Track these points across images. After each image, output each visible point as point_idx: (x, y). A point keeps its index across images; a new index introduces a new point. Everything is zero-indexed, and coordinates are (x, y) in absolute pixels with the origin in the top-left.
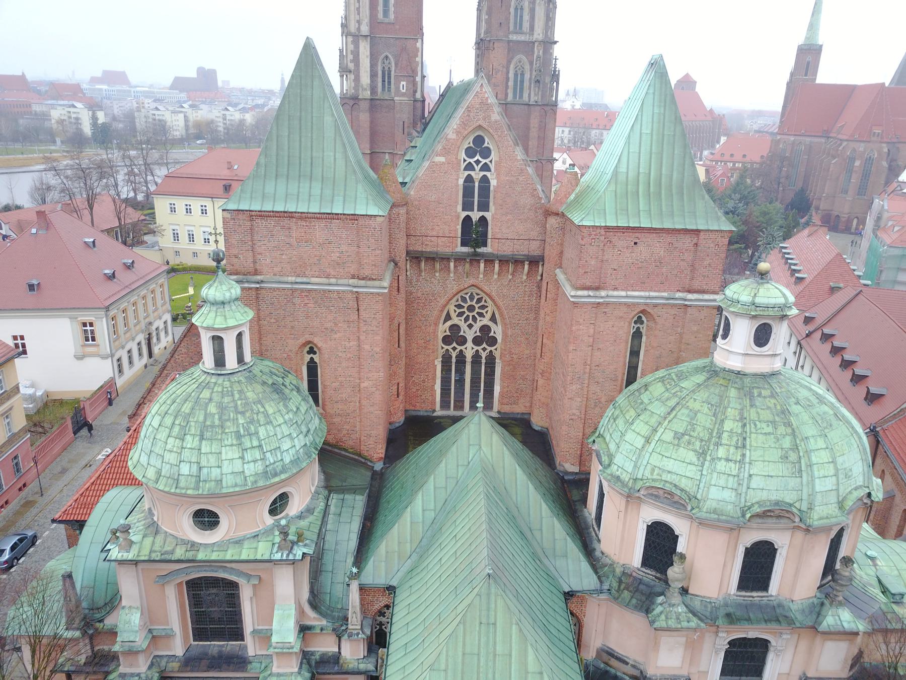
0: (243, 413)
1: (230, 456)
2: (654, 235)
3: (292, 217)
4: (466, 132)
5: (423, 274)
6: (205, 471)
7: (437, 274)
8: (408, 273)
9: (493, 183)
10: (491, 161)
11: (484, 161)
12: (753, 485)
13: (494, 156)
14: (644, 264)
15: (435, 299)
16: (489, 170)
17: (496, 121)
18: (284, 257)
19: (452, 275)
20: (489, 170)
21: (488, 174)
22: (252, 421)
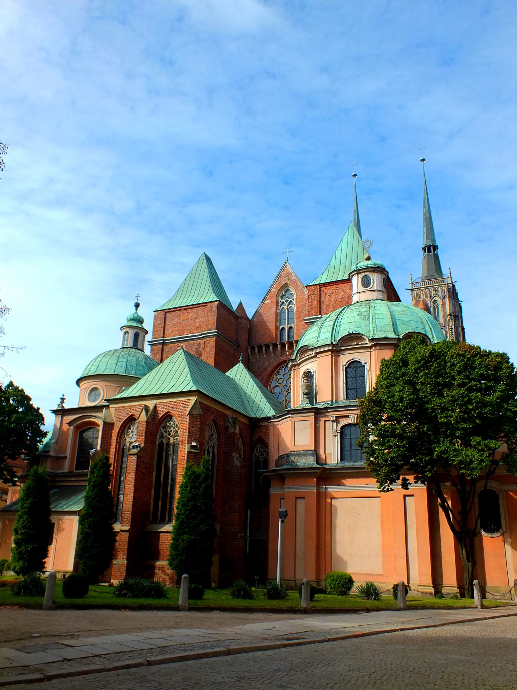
0: (124, 352)
1: (111, 363)
2: (345, 284)
3: (181, 310)
4: (280, 287)
5: (258, 357)
6: (99, 367)
7: (265, 356)
8: (250, 358)
9: (295, 309)
10: (294, 300)
11: (290, 300)
12: (342, 328)
13: (295, 297)
14: (342, 300)
15: (265, 371)
16: (293, 304)
17: (294, 280)
18: (176, 328)
19: (272, 355)
20: (293, 304)
21: (293, 306)
22: (126, 354)
